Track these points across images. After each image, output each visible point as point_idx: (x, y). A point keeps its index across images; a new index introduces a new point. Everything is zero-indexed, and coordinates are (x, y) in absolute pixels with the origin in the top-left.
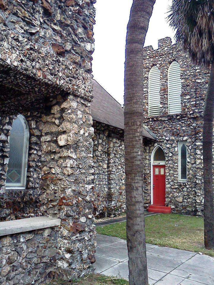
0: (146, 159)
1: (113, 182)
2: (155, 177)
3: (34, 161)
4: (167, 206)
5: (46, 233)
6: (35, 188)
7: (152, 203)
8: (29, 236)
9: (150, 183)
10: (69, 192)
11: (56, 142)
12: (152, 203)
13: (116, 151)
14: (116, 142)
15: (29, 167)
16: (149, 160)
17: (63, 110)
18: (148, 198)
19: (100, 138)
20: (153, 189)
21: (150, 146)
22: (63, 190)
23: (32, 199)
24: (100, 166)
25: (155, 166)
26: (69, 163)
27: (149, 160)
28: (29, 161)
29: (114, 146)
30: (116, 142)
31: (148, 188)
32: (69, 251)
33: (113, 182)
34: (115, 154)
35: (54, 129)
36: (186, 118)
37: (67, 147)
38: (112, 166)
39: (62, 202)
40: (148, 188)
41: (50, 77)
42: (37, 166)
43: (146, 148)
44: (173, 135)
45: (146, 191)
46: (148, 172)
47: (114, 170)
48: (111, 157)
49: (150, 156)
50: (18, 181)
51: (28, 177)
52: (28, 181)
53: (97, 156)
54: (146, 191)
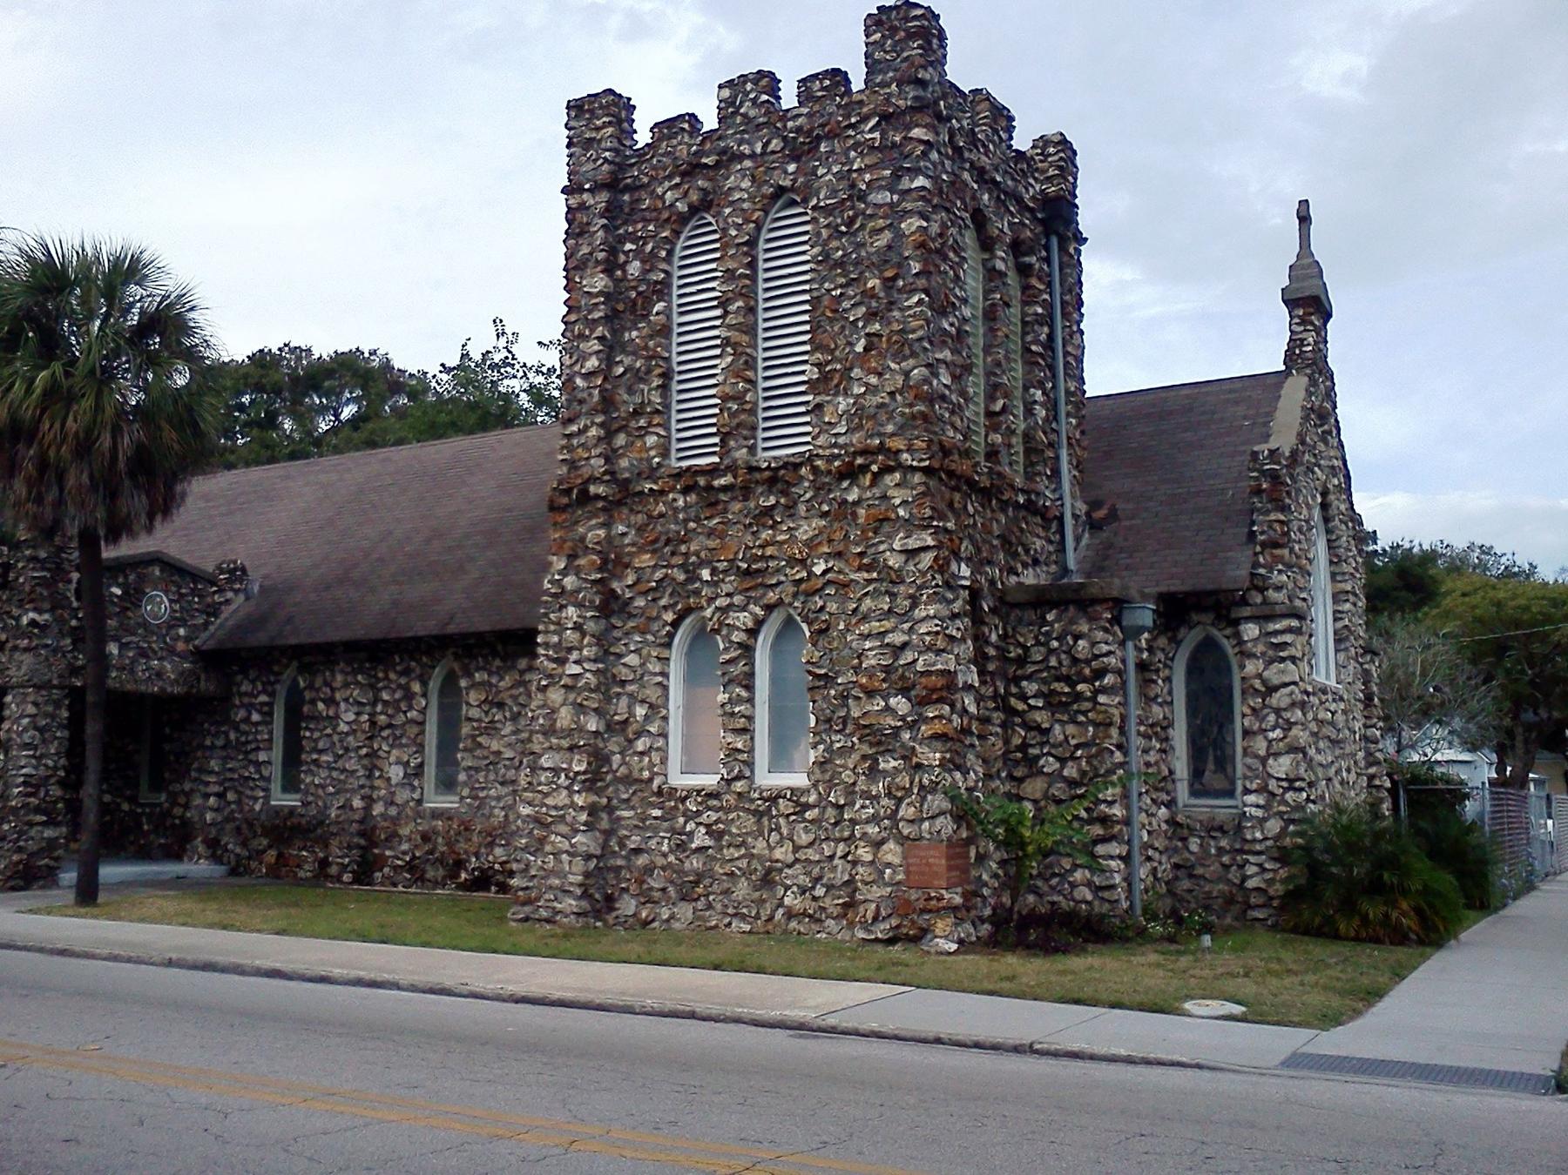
24: (480, 745)
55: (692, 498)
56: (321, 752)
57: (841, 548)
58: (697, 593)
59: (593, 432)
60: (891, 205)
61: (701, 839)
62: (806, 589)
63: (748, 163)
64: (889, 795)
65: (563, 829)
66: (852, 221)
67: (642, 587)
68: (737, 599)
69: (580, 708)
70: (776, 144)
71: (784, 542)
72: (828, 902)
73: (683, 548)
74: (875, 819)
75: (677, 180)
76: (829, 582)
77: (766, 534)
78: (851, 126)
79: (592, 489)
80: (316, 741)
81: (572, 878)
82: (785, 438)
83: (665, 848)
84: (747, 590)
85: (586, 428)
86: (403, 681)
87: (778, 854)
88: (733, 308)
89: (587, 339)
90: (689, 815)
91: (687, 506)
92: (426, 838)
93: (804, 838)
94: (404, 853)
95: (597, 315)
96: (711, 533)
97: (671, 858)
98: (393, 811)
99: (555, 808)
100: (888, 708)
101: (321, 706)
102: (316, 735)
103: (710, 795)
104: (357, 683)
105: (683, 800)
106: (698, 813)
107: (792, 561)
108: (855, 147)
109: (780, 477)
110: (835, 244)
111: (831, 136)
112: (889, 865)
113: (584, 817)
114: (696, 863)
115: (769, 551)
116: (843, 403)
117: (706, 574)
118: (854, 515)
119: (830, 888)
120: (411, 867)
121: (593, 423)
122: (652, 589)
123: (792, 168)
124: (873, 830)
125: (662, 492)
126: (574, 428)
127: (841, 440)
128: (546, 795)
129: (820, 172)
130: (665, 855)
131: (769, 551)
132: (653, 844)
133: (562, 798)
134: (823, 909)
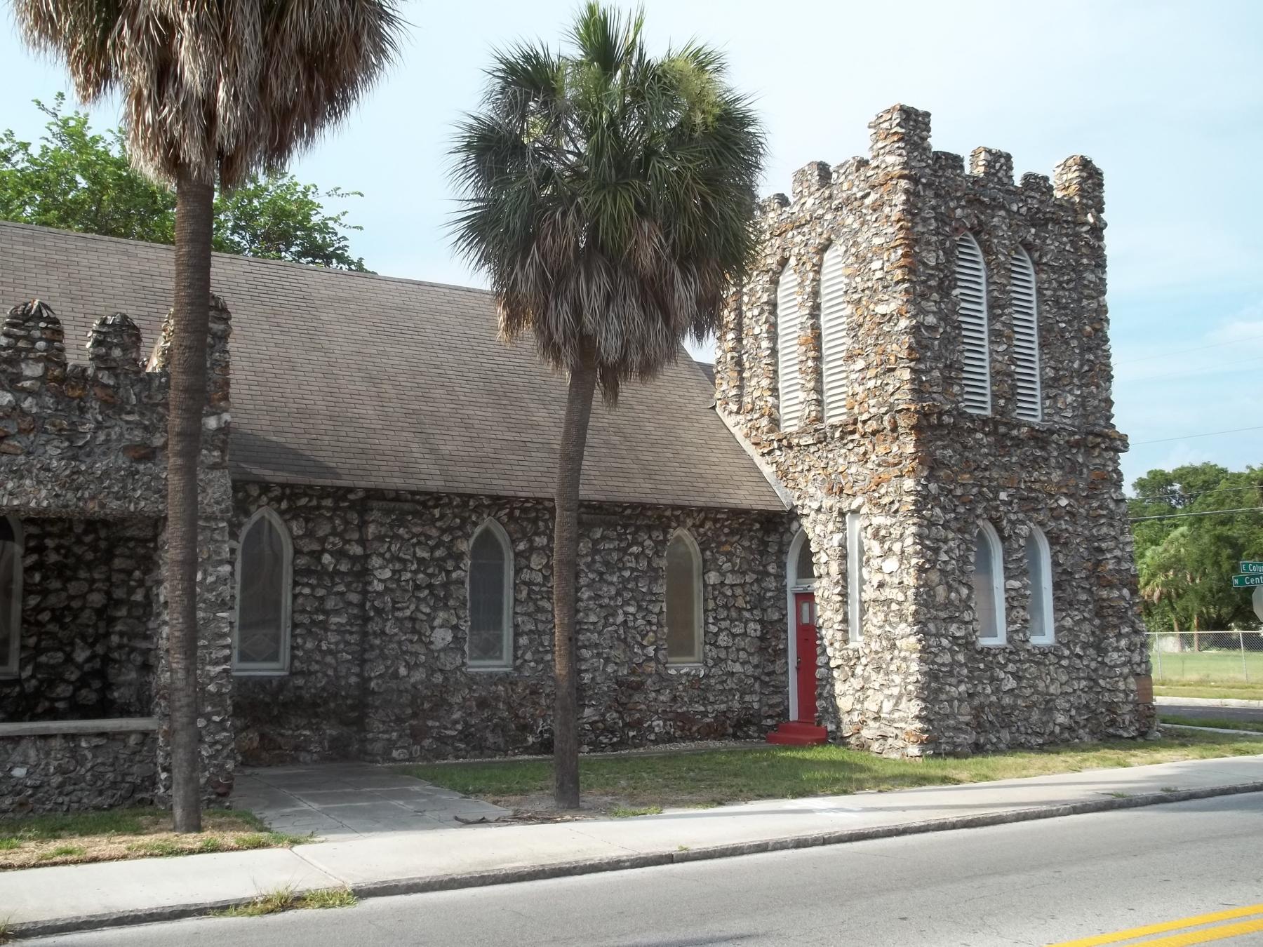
0: (768, 574)
1: (586, 653)
3: (304, 611)
4: (819, 724)
5: (133, 740)
6: (310, 673)
7: (793, 715)
8: (95, 741)
9: (785, 650)
12: (793, 715)
13: (607, 564)
14: (603, 538)
15: (295, 626)
16: (781, 577)
19: (537, 534)
21: (781, 530)
23: (300, 698)
24: (539, 610)
27: (776, 576)
28: (294, 612)
29: (595, 551)
30: (603, 538)
33: (586, 653)
34: (601, 574)
36: (857, 436)
38: (587, 609)
40: (778, 667)
41: (115, 504)
42: (313, 622)
43: (766, 539)
44: (830, 491)
45: (767, 679)
46: (776, 616)
47: (593, 619)
48: (583, 581)
49: (782, 566)
50: (274, 657)
51: (293, 648)
52: (293, 657)
53: (529, 584)
54: (767, 679)
55: (991, 439)
56: (327, 613)
57: (1073, 490)
58: (996, 509)
59: (936, 373)
60: (1095, 283)
61: (1011, 684)
62: (1055, 514)
63: (1002, 213)
64: (1129, 649)
65: (954, 681)
66: (1068, 282)
67: (964, 499)
68: (1021, 516)
69: (950, 588)
70: (1024, 210)
71: (1044, 482)
72: (1078, 719)
73: (987, 474)
74: (1124, 664)
75: (963, 203)
76: (1068, 512)
77: (1036, 474)
78: (1067, 222)
79: (945, 418)
80: (322, 599)
81: (962, 719)
82: (1033, 410)
83: (989, 690)
84: (1028, 510)
85: (932, 369)
86: (446, 538)
87: (1052, 690)
88: (1007, 311)
89: (928, 300)
90: (1003, 667)
91: (989, 446)
92: (482, 704)
93: (1064, 678)
94: (456, 722)
95: (933, 283)
96: (1005, 467)
97: (994, 698)
98: (438, 678)
99: (943, 665)
100: (1122, 597)
101: (327, 558)
102: (321, 592)
103: (1011, 653)
104: (396, 537)
105: (995, 656)
106: (1006, 665)
107: (1051, 496)
108: (1067, 235)
109: (1040, 438)
110: (1061, 293)
111: (1056, 222)
112: (1132, 691)
113: (965, 671)
114: (1007, 700)
115: (1037, 486)
116: (1070, 399)
117: (1003, 496)
118: (1081, 473)
119: (1077, 709)
120: (465, 736)
121: (936, 367)
122: (971, 501)
123: (1033, 231)
124: (1126, 670)
125: (975, 431)
126: (922, 366)
127: (1067, 421)
128: (936, 655)
129: (1048, 242)
130: (988, 696)
131: (1037, 486)
132: (979, 688)
133: (947, 658)
134: (1076, 723)
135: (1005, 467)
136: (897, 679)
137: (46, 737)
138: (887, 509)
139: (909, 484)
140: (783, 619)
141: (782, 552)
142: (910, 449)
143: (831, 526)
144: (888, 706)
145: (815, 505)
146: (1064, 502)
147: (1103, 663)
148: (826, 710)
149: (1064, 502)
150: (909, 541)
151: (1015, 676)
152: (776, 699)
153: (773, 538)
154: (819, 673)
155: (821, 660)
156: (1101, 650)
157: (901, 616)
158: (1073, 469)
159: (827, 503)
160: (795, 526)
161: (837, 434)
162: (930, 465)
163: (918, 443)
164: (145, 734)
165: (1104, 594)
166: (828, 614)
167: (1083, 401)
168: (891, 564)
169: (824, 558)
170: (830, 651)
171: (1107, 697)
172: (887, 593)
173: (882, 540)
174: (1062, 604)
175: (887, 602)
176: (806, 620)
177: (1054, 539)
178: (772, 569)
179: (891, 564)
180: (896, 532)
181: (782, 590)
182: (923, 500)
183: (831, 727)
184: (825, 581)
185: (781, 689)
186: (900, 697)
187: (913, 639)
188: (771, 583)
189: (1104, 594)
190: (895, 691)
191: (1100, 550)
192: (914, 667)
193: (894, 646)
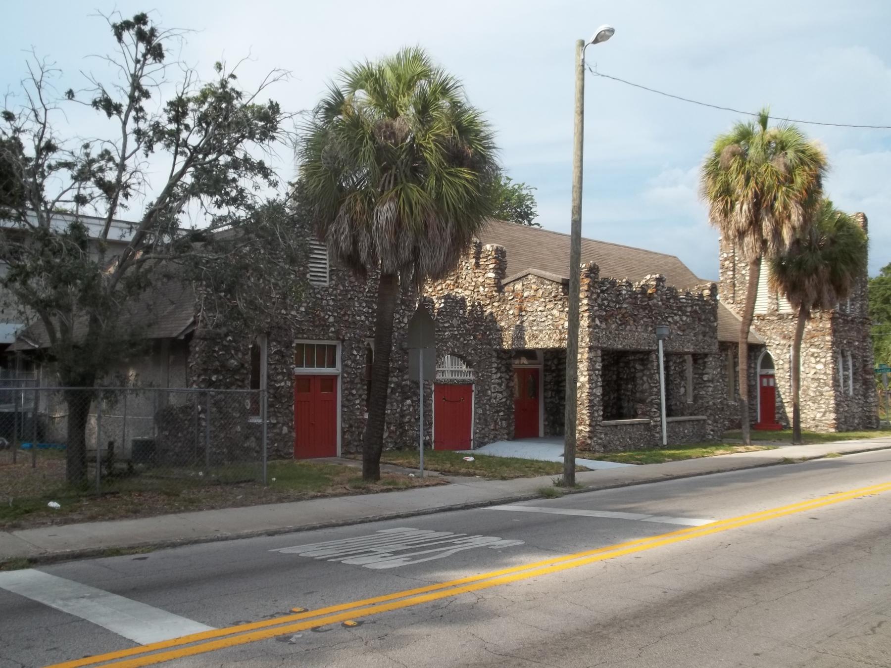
2: (762, 388)
7: (759, 421)
10: (711, 403)
11: (702, 378)
12: (759, 421)
16: (755, 368)
17: (705, 363)
18: (754, 414)
20: (761, 403)
22: (708, 402)
25: (762, 376)
26: (711, 389)
31: (754, 402)
32: (712, 430)
35: (700, 371)
37: (709, 381)
39: (707, 408)
44: (784, 338)
49: (756, 364)
61: (847, 409)
96: (845, 331)
135: (845, 331)
136: (823, 406)
137: (693, 421)
138: (817, 346)
139: (828, 338)
140: (756, 384)
141: (756, 358)
142: (829, 326)
143: (785, 351)
144: (819, 416)
145: (777, 343)
146: (857, 343)
147: (866, 402)
148: (781, 418)
149: (857, 343)
150: (829, 358)
151: (848, 406)
152: (754, 414)
153: (753, 354)
154: (777, 404)
155: (778, 400)
156: (865, 396)
157: (826, 384)
158: (859, 331)
159: (783, 342)
160: (763, 349)
161: (790, 317)
162: (834, 331)
163: (832, 324)
164: (704, 420)
165: (868, 377)
166: (782, 383)
167: (862, 305)
168: (820, 366)
169: (781, 362)
170: (783, 396)
171: (867, 414)
172: (816, 377)
173: (816, 357)
174: (855, 380)
175: (819, 379)
176: (765, 384)
177: (853, 357)
178: (753, 365)
179: (820, 366)
180: (822, 355)
181: (755, 373)
182: (833, 344)
183: (784, 424)
184: (781, 371)
185: (755, 411)
186: (824, 413)
187: (832, 393)
188: (752, 371)
189: (868, 377)
190: (823, 410)
191: (866, 361)
192: (832, 402)
193: (822, 395)
